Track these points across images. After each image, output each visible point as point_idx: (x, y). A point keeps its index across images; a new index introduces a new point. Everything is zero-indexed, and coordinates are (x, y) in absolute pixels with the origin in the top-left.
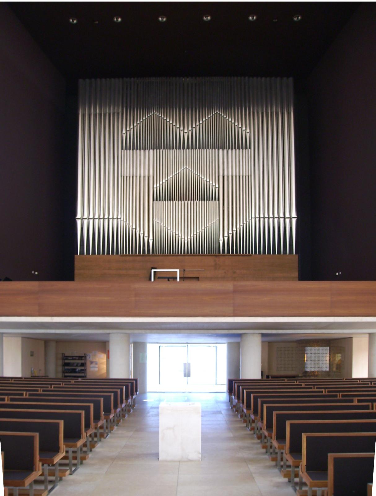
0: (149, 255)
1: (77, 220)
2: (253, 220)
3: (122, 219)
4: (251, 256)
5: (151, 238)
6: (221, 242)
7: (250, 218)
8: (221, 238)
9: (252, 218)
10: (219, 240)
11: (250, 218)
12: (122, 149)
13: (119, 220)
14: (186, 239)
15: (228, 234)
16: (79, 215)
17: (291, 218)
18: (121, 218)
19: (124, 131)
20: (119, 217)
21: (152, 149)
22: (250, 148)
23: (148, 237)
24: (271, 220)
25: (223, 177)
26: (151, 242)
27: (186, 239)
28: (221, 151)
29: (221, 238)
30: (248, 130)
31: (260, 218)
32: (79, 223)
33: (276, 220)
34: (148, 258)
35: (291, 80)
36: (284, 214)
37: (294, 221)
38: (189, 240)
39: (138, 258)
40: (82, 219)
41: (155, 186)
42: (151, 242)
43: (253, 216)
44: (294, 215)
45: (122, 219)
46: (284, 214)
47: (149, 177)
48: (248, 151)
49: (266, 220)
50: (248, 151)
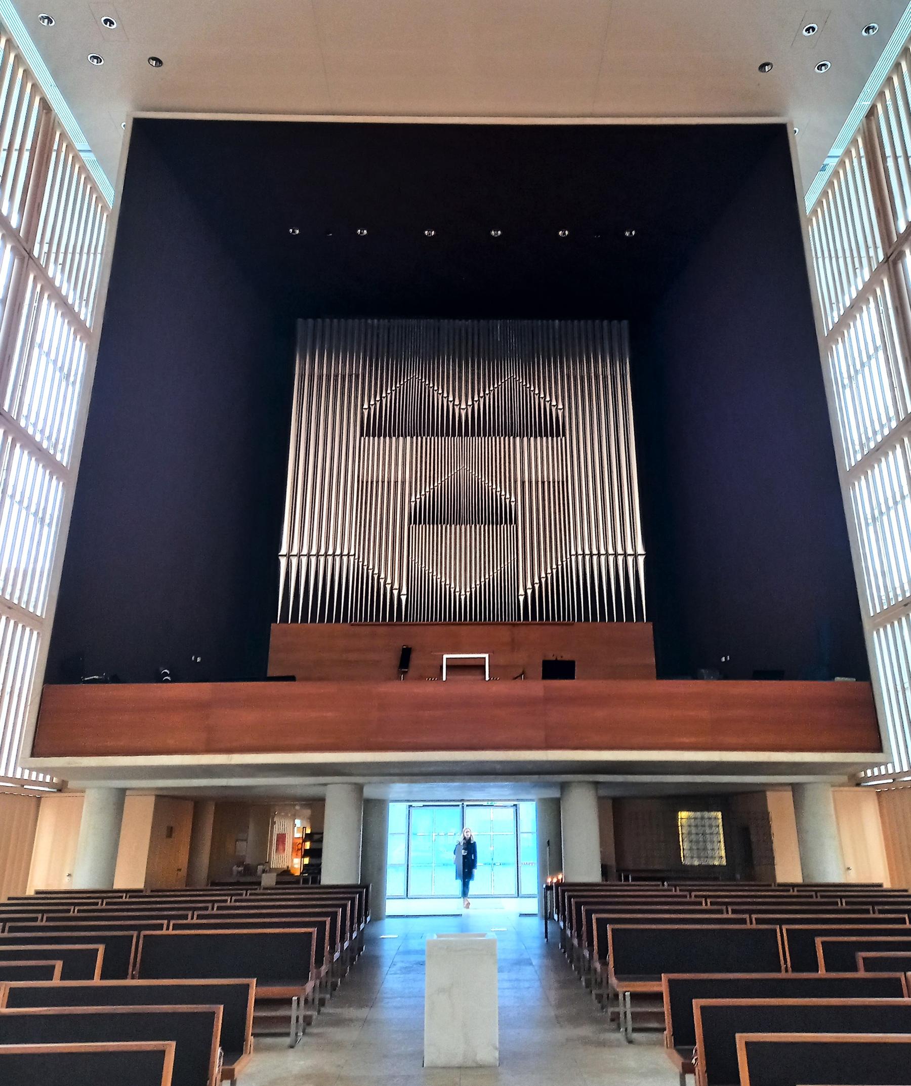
0: (401, 623)
1: (280, 558)
2: (573, 558)
3: (357, 557)
4: (572, 624)
5: (404, 591)
6: (521, 598)
7: (568, 556)
8: (521, 592)
9: (571, 555)
10: (518, 596)
11: (568, 556)
12: (362, 435)
13: (352, 558)
14: (463, 593)
15: (533, 584)
16: (284, 550)
17: (635, 556)
18: (355, 555)
19: (366, 406)
20: (352, 553)
21: (409, 436)
22: (564, 435)
23: (400, 590)
24: (603, 558)
25: (523, 483)
26: (404, 598)
27: (463, 593)
28: (518, 439)
29: (521, 592)
30: (560, 406)
31: (584, 555)
32: (283, 561)
33: (611, 558)
34: (398, 628)
35: (625, 323)
36: (625, 549)
37: (641, 560)
38: (468, 594)
39: (382, 630)
40: (289, 556)
41: (413, 499)
42: (404, 598)
43: (573, 552)
44: (640, 549)
45: (357, 557)
46: (625, 549)
47: (403, 483)
48: (561, 440)
49: (595, 558)
50: (561, 440)
